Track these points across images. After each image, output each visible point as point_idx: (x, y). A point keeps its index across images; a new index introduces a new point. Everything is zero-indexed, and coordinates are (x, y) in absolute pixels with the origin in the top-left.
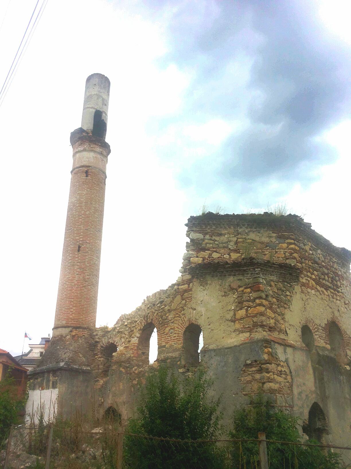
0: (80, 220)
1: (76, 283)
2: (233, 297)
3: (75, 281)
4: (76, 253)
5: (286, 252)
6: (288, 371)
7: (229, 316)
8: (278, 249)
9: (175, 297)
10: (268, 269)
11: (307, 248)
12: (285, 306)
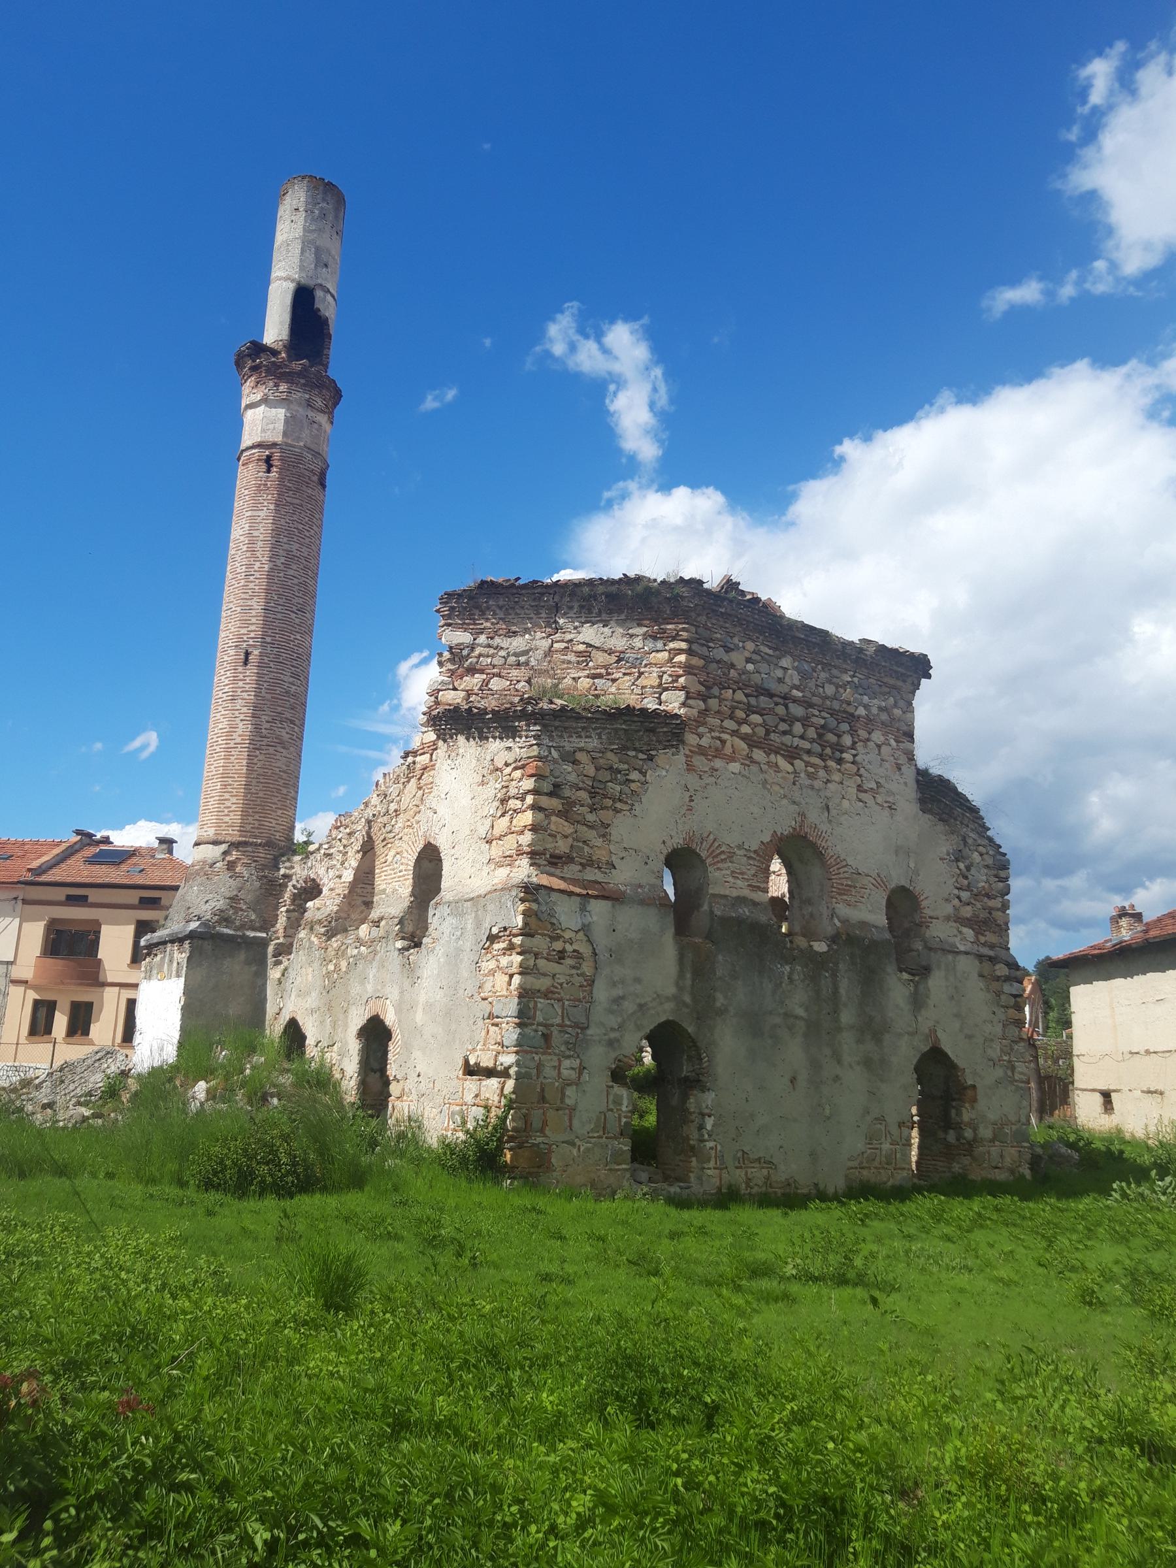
0: (251, 585)
1: (239, 740)
2: (493, 788)
3: (235, 736)
4: (240, 669)
5: (664, 673)
6: (585, 950)
7: (482, 831)
8: (646, 666)
9: (408, 782)
10: (567, 724)
11: (737, 658)
12: (619, 805)
